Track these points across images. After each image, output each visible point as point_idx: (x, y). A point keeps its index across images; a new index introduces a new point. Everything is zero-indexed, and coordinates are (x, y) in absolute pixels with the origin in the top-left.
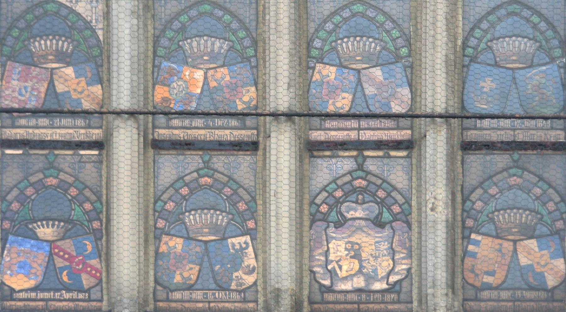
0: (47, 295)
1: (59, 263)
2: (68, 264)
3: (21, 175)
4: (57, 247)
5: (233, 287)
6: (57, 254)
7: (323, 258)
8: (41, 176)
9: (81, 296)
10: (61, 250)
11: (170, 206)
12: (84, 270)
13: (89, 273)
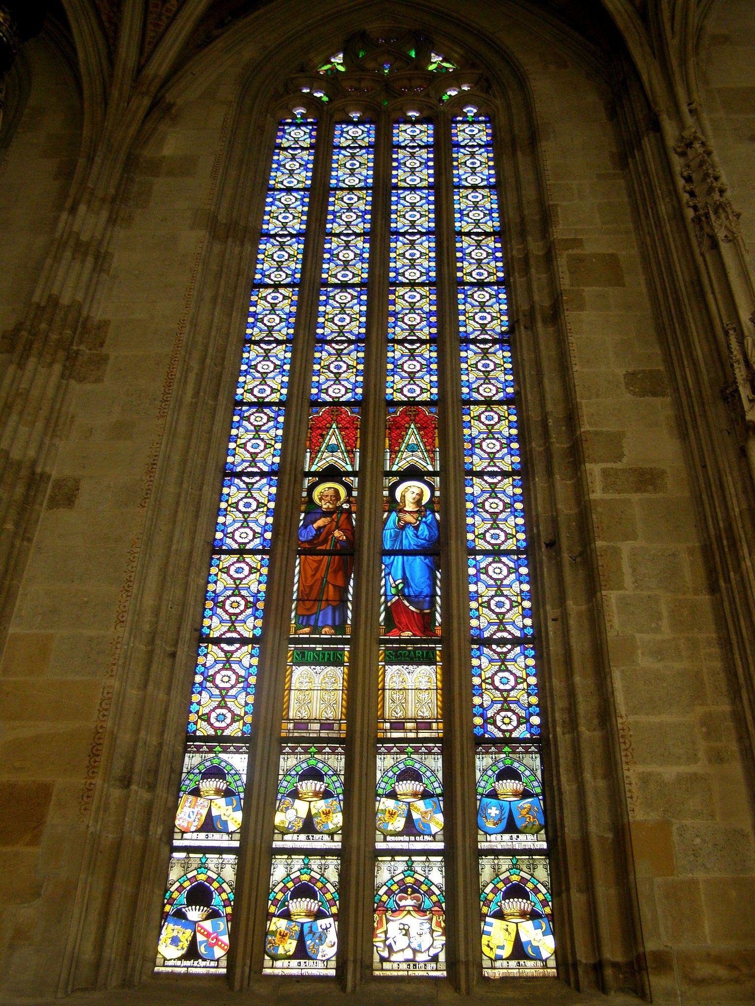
0: (188, 963)
1: (200, 938)
2: (206, 939)
3: (182, 873)
4: (199, 926)
5: (319, 957)
6: (199, 932)
7: (383, 935)
8: (195, 873)
9: (213, 964)
10: (202, 928)
11: (280, 896)
12: (216, 944)
13: (220, 946)
